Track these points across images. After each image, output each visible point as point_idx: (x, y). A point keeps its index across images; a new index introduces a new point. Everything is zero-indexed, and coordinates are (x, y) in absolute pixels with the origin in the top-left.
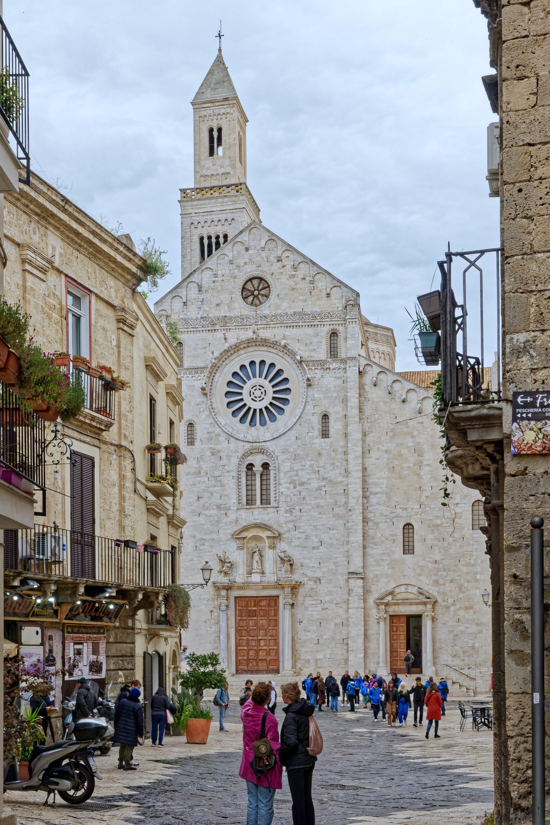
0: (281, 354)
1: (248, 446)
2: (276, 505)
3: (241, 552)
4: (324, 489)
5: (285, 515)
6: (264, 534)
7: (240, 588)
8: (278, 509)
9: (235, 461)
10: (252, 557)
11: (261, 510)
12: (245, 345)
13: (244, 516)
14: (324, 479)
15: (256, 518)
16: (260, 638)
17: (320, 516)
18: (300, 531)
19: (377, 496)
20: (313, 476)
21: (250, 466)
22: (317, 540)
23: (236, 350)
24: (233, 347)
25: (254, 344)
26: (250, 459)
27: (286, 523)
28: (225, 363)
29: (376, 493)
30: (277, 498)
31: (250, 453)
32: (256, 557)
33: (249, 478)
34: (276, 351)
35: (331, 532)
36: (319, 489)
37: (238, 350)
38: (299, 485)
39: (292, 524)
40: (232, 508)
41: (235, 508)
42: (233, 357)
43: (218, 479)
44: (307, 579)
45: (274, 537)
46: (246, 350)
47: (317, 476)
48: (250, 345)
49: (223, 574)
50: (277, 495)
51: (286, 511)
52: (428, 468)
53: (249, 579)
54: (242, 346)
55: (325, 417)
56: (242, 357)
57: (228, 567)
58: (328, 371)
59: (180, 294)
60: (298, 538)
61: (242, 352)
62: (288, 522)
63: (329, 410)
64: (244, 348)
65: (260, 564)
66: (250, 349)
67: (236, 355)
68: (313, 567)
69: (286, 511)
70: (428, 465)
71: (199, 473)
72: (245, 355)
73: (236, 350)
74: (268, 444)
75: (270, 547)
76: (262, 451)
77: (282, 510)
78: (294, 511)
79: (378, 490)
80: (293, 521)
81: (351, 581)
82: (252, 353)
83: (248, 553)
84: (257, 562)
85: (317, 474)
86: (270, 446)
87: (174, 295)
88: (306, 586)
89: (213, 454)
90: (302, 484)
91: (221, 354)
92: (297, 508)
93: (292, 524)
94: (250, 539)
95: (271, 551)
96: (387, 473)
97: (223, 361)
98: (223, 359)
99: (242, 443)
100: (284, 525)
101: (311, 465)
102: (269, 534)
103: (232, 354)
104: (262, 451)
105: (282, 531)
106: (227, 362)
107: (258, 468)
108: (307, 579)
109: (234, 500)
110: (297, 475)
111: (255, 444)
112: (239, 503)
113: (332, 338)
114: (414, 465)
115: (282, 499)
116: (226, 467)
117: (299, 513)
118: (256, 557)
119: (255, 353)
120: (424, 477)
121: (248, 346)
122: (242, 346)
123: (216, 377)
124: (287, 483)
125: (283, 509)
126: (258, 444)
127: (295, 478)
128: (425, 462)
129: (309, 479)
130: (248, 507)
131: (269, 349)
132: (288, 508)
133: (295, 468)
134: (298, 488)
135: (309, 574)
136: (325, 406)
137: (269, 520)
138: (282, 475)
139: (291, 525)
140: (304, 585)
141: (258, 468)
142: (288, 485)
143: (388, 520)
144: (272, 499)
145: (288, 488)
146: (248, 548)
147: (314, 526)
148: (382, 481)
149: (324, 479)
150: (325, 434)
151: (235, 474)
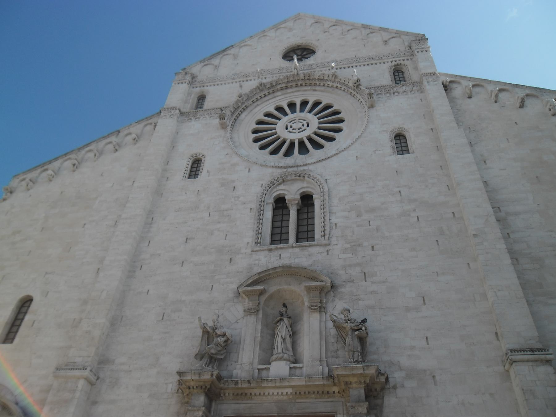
0: (331, 89)
1: (279, 171)
2: (324, 242)
3: (252, 319)
5: (341, 256)
8: (328, 248)
9: (256, 190)
10: (273, 335)
11: (297, 250)
12: (283, 85)
23: (271, 91)
24: (268, 86)
25: (294, 84)
26: (281, 190)
27: (344, 267)
28: (255, 104)
30: (327, 232)
31: (283, 181)
32: (283, 331)
33: (279, 218)
34: (323, 88)
37: (274, 92)
39: (358, 269)
40: (243, 251)
41: (249, 251)
42: (267, 98)
44: (403, 374)
45: (321, 289)
46: (284, 92)
48: (289, 85)
49: (205, 360)
50: (327, 228)
51: (345, 250)
53: (264, 374)
54: (279, 87)
56: (278, 98)
57: (217, 345)
58: (396, 94)
59: (213, 62)
60: (372, 293)
61: (279, 93)
62: (350, 266)
63: (405, 126)
64: (282, 89)
65: (289, 346)
66: (289, 91)
67: (271, 96)
68: (413, 348)
69: (345, 250)
72: (283, 97)
73: (271, 91)
74: (311, 167)
75: (313, 308)
76: (302, 176)
80: (359, 264)
81: (516, 368)
82: (292, 94)
83: (266, 325)
84: (284, 339)
87: (205, 63)
88: (400, 392)
89: (223, 185)
90: (372, 210)
91: (252, 91)
92: (366, 244)
93: (358, 269)
94: (271, 297)
95: (316, 316)
97: (253, 102)
98: (254, 99)
100: (342, 272)
102: (313, 284)
103: (265, 96)
105: (337, 282)
106: (259, 102)
108: (403, 374)
109: (249, 237)
112: (257, 243)
113: (396, 74)
116: (241, 199)
117: (370, 252)
118: (283, 331)
119: (296, 94)
121: (287, 88)
122: (279, 87)
123: (243, 116)
126: (295, 169)
130: (273, 247)
131: (314, 88)
132: (348, 246)
135: (405, 361)
136: (397, 124)
138: (335, 202)
140: (395, 387)
144: (317, 235)
146: (265, 315)
151: (254, 205)
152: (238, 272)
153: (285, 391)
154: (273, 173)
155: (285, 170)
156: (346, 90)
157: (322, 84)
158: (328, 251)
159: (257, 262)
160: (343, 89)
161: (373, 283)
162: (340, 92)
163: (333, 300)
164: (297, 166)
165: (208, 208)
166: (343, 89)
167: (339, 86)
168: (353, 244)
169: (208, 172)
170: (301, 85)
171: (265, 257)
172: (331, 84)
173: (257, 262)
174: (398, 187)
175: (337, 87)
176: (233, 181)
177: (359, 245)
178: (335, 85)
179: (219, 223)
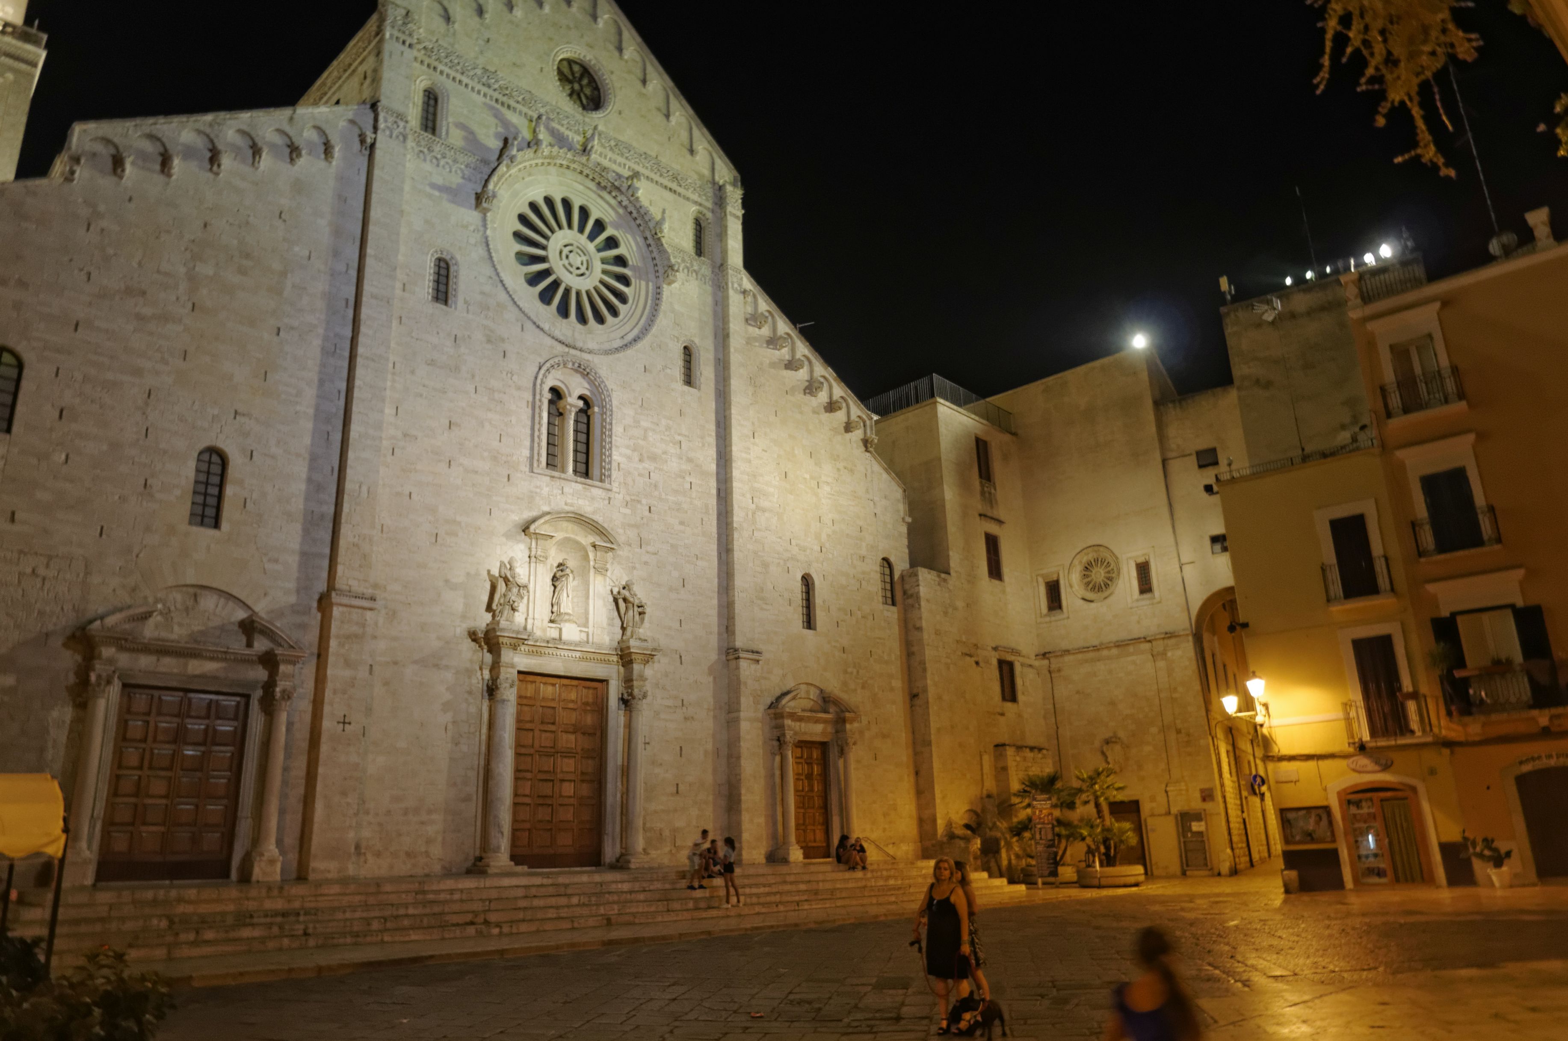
2: (607, 485)
4: (688, 479)
5: (623, 510)
6: (586, 539)
7: (536, 651)
8: (611, 495)
13: (546, 490)
14: (690, 460)
15: (569, 501)
16: (560, 776)
17: (682, 528)
18: (651, 549)
19: (767, 514)
20: (673, 450)
21: (557, 394)
22: (675, 574)
29: (764, 510)
35: (699, 563)
36: (681, 475)
38: (649, 457)
43: (497, 396)
47: (678, 450)
52: (827, 489)
55: (688, 352)
70: (828, 483)
71: (457, 369)
77: (619, 498)
78: (639, 506)
79: (765, 504)
80: (636, 526)
85: (678, 446)
86: (602, 366)
90: (653, 458)
92: (644, 501)
95: (599, 578)
96: (778, 479)
99: (549, 341)
100: (621, 531)
101: (668, 428)
104: (584, 371)
107: (573, 403)
110: (645, 438)
111: (572, 352)
114: (812, 478)
115: (615, 474)
116: (515, 378)
117: (647, 513)
120: (823, 501)
124: (628, 447)
125: (620, 497)
127: (641, 442)
128: (824, 478)
129: (665, 453)
132: (628, 498)
133: (644, 424)
134: (648, 465)
137: (594, 513)
139: (632, 534)
141: (573, 403)
142: (629, 452)
143: (782, 562)
145: (629, 458)
147: (672, 546)
148: (771, 490)
149: (690, 460)
150: (689, 380)
152: (518, 498)
153: (574, 654)
154: (552, 347)
155: (567, 349)
156: (641, 228)
157: (614, 194)
158: (610, 499)
159: (538, 490)
160: (638, 222)
161: (648, 552)
162: (632, 223)
163: (612, 563)
164: (581, 350)
165: (473, 376)
166: (638, 222)
167: (635, 214)
168: (633, 498)
169: (466, 302)
170: (587, 176)
171: (547, 486)
172: (625, 203)
173: (538, 490)
174: (679, 434)
175: (631, 213)
176: (503, 340)
177: (639, 502)
178: (631, 208)
179: (490, 410)
